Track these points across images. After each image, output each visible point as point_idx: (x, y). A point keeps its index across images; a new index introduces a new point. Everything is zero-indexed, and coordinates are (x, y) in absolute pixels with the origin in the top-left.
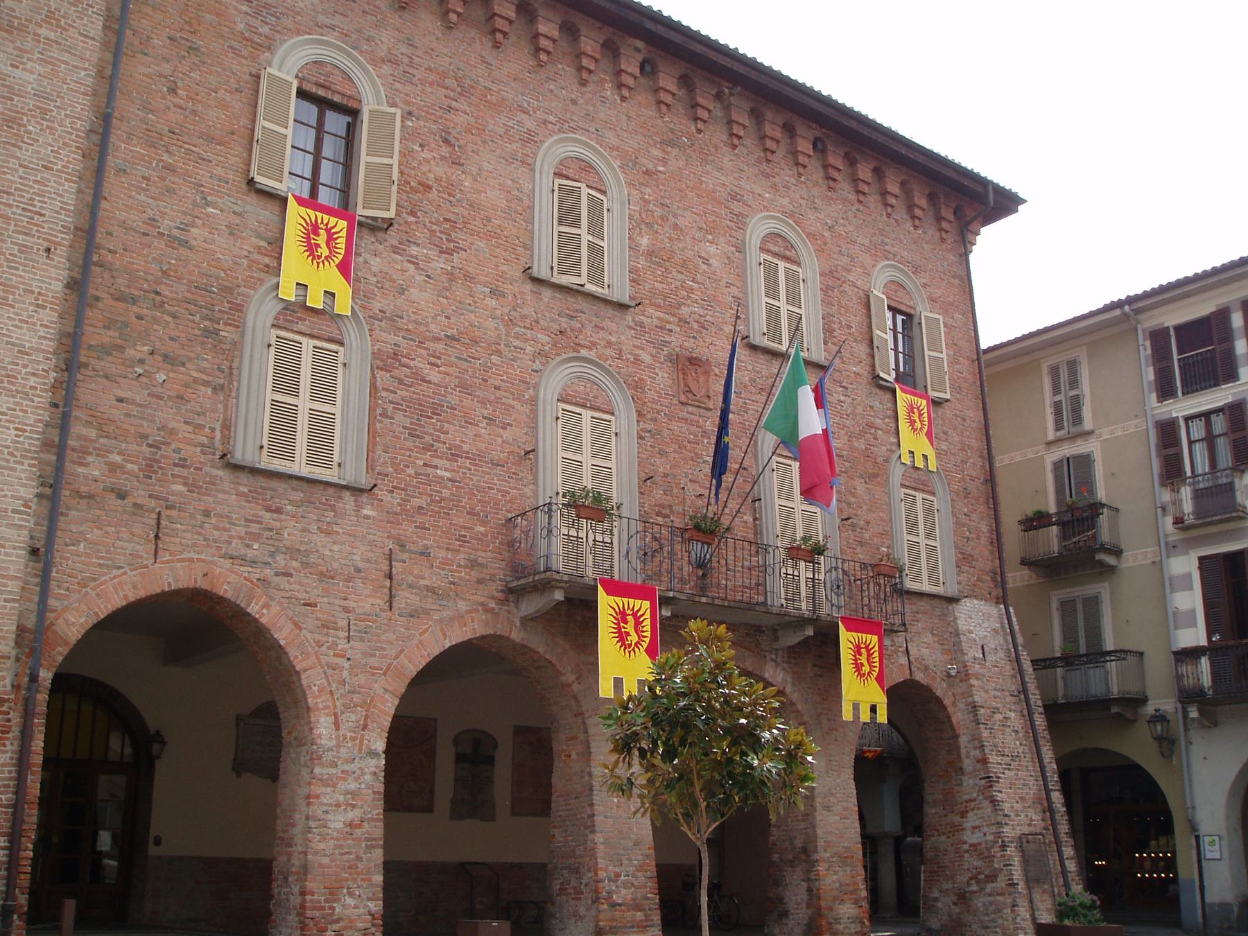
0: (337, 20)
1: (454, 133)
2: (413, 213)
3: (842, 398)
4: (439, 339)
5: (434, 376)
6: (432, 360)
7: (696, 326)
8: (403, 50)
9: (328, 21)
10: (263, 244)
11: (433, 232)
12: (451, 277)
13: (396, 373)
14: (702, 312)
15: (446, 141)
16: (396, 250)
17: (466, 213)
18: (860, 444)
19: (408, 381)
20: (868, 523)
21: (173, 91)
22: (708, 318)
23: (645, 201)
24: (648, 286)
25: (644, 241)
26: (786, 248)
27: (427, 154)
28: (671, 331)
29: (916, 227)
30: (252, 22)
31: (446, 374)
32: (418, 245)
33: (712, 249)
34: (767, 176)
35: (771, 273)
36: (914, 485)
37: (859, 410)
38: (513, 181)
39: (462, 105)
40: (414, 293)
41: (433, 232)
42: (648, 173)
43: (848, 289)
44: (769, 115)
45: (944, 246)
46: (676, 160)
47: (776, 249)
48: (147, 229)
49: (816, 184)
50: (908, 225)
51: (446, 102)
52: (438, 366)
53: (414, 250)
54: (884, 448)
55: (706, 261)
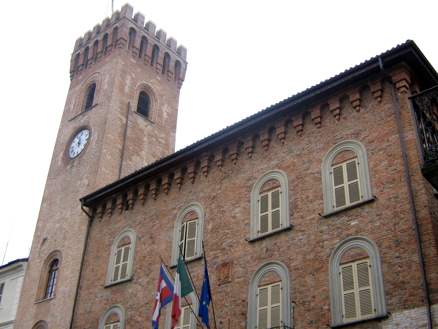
0: (129, 222)
1: (154, 233)
2: (141, 268)
3: (301, 237)
4: (142, 306)
5: (140, 319)
6: (140, 314)
7: (228, 248)
8: (143, 217)
9: (125, 225)
10: (106, 302)
11: (145, 271)
12: (148, 283)
13: (131, 324)
14: (231, 240)
15: (151, 238)
16: (136, 283)
17: (154, 258)
18: (312, 256)
19: (133, 324)
20: (314, 297)
21: (93, 272)
22: (234, 241)
23: (211, 210)
24: (210, 244)
25: (210, 227)
26: (275, 183)
27: (146, 246)
28: (218, 257)
29: (358, 111)
30: (110, 239)
31: (143, 317)
32: (141, 278)
33: (237, 210)
34: (265, 158)
35: (264, 200)
36: (351, 259)
37: (313, 237)
38: (169, 237)
39: (157, 222)
40: (139, 295)
41: (145, 271)
42: (214, 198)
43: (307, 179)
44: (262, 132)
45: (382, 104)
46: (226, 183)
47: (268, 188)
48: (84, 312)
49: (293, 139)
50: (355, 113)
51: (152, 225)
52: (141, 315)
53: (140, 280)
54: (328, 249)
55: (234, 217)
